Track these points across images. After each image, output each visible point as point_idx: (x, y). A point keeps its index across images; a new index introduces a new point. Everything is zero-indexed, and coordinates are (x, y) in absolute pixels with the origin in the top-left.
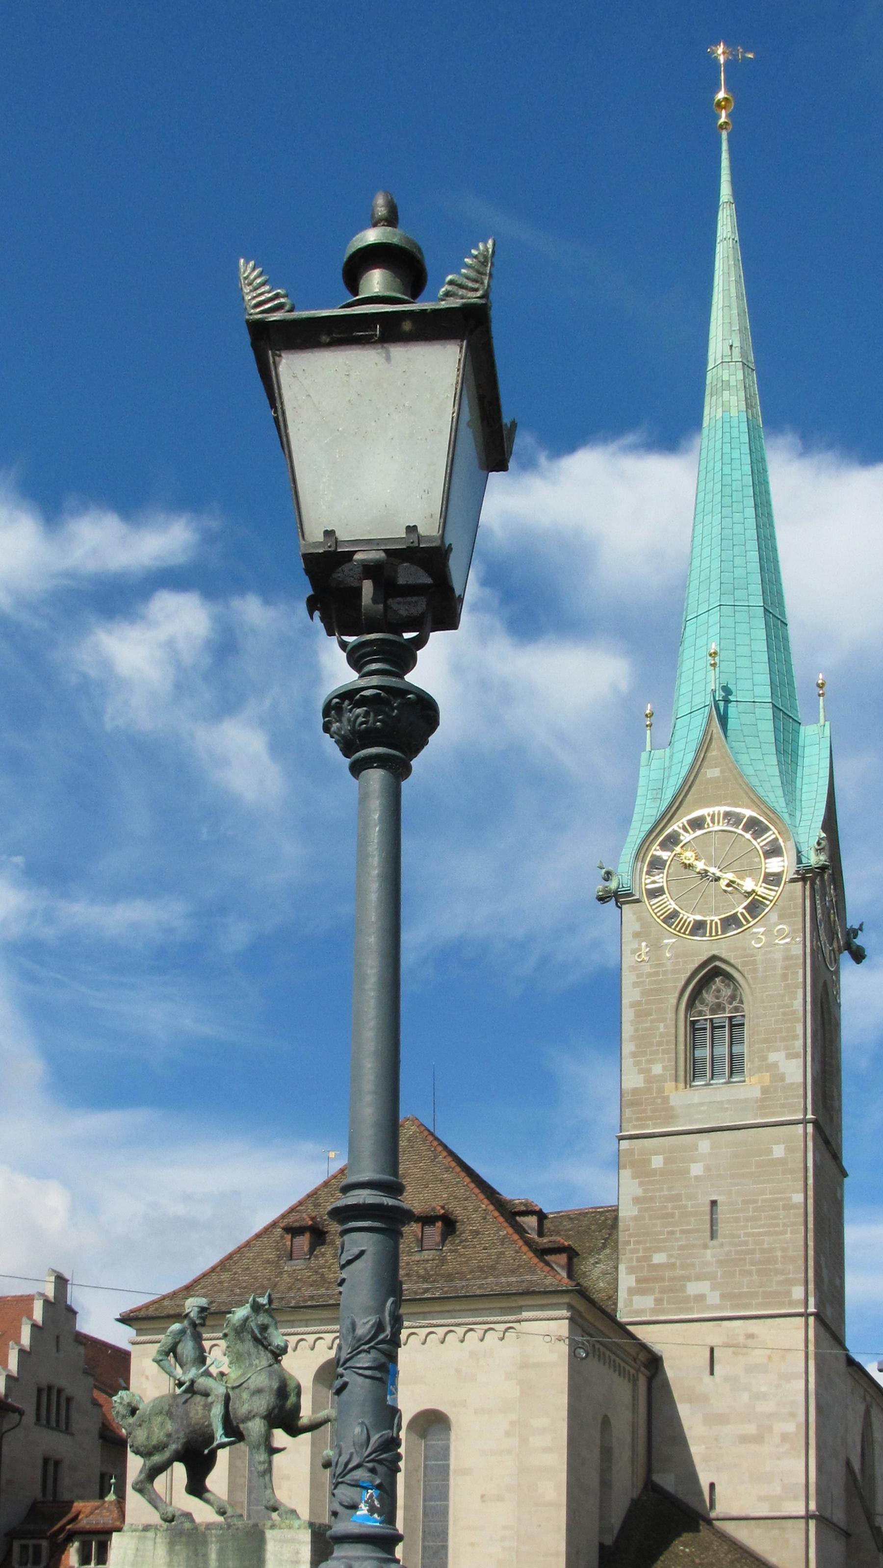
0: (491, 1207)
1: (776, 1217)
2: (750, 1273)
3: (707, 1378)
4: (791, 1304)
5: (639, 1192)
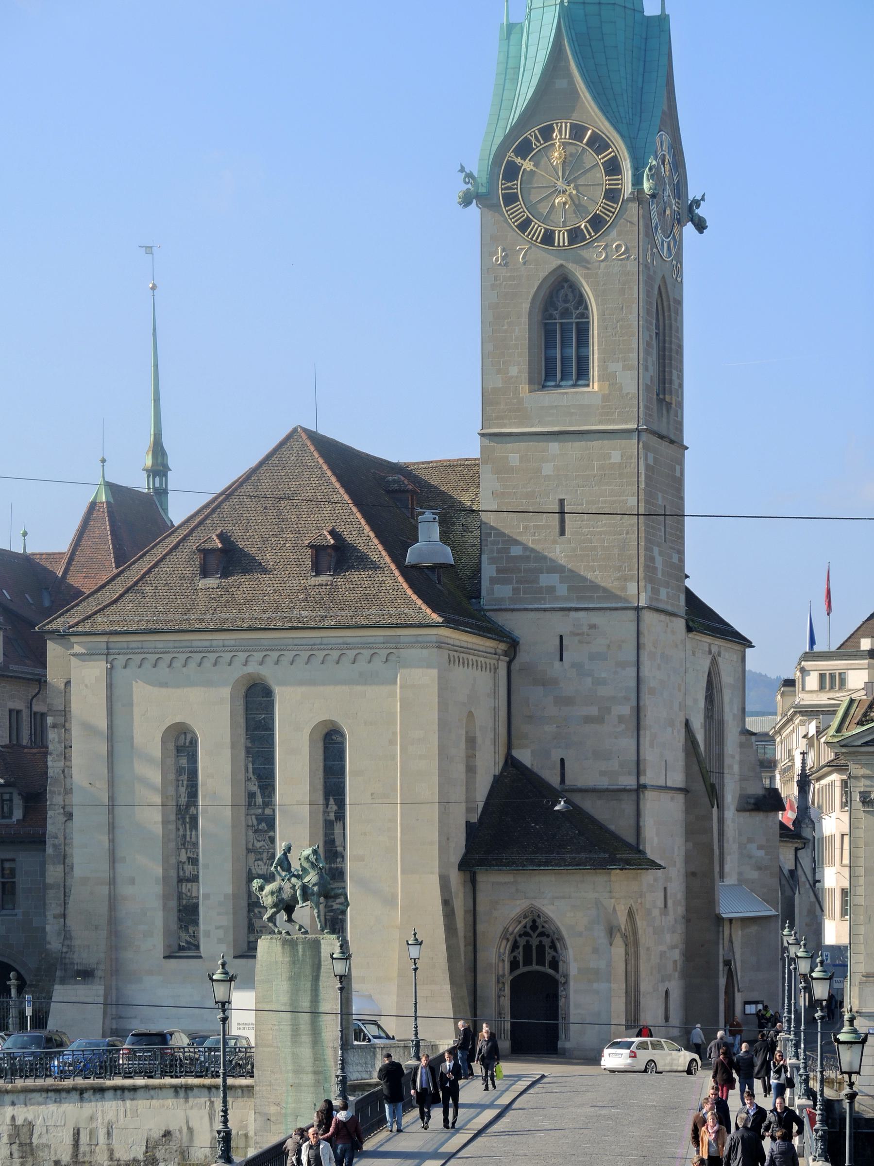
0: (372, 534)
3: (557, 664)
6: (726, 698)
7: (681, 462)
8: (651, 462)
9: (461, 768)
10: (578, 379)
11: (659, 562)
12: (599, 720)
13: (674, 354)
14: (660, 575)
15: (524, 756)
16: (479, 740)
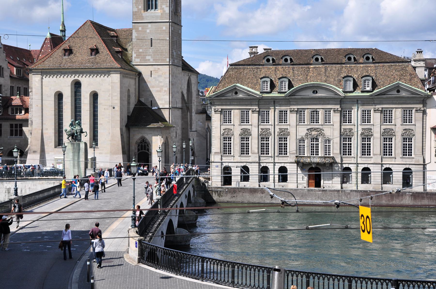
0: (105, 46)
1: (164, 43)
2: (158, 55)
4: (167, 62)
5: (137, 35)
6: (193, 87)
7: (181, 30)
8: (173, 29)
9: (126, 103)
10: (155, 9)
11: (175, 54)
12: (160, 91)
13: (179, 4)
14: (175, 57)
15: (142, 100)
16: (131, 96)
